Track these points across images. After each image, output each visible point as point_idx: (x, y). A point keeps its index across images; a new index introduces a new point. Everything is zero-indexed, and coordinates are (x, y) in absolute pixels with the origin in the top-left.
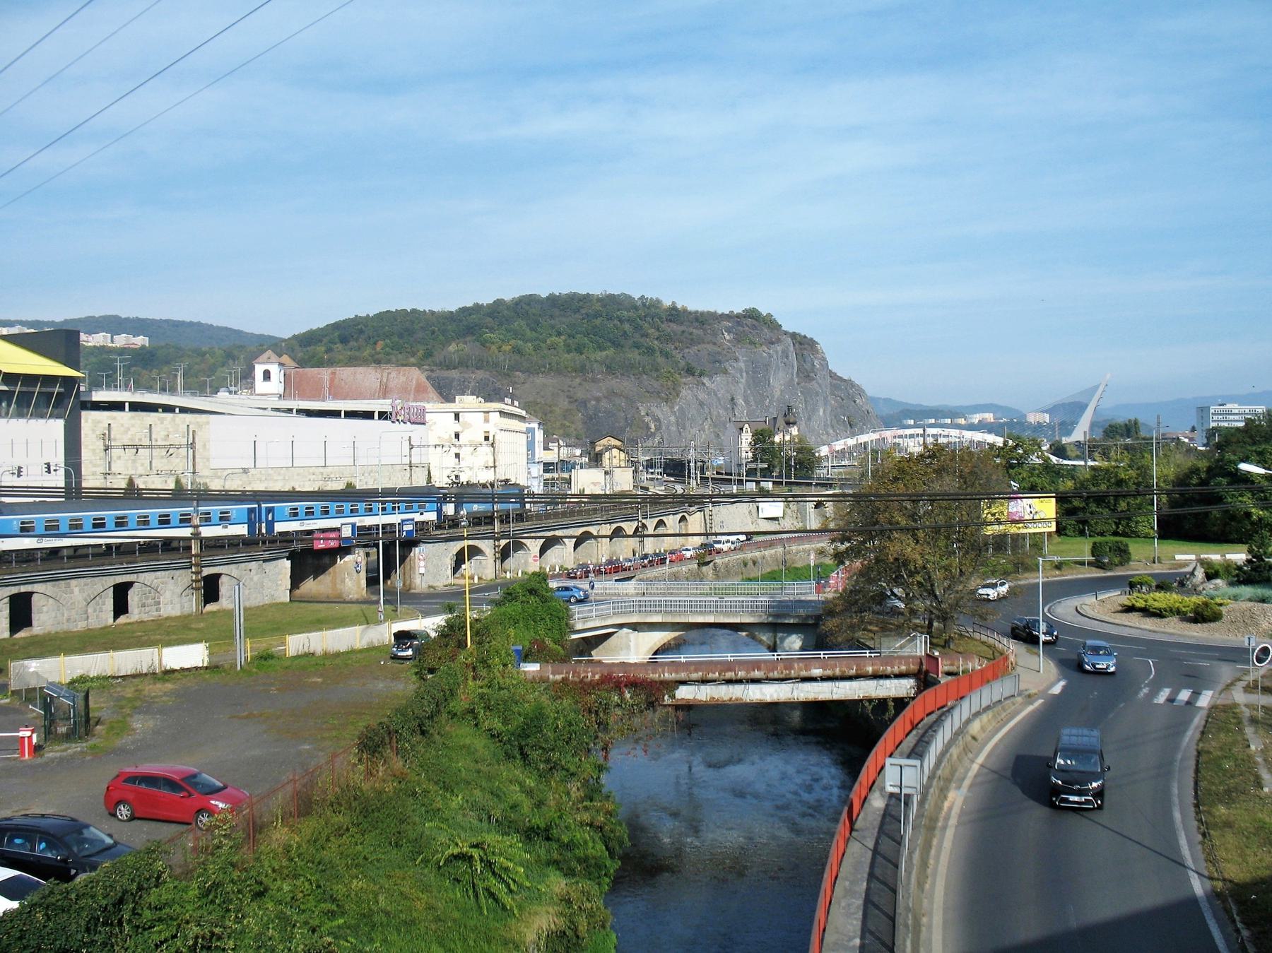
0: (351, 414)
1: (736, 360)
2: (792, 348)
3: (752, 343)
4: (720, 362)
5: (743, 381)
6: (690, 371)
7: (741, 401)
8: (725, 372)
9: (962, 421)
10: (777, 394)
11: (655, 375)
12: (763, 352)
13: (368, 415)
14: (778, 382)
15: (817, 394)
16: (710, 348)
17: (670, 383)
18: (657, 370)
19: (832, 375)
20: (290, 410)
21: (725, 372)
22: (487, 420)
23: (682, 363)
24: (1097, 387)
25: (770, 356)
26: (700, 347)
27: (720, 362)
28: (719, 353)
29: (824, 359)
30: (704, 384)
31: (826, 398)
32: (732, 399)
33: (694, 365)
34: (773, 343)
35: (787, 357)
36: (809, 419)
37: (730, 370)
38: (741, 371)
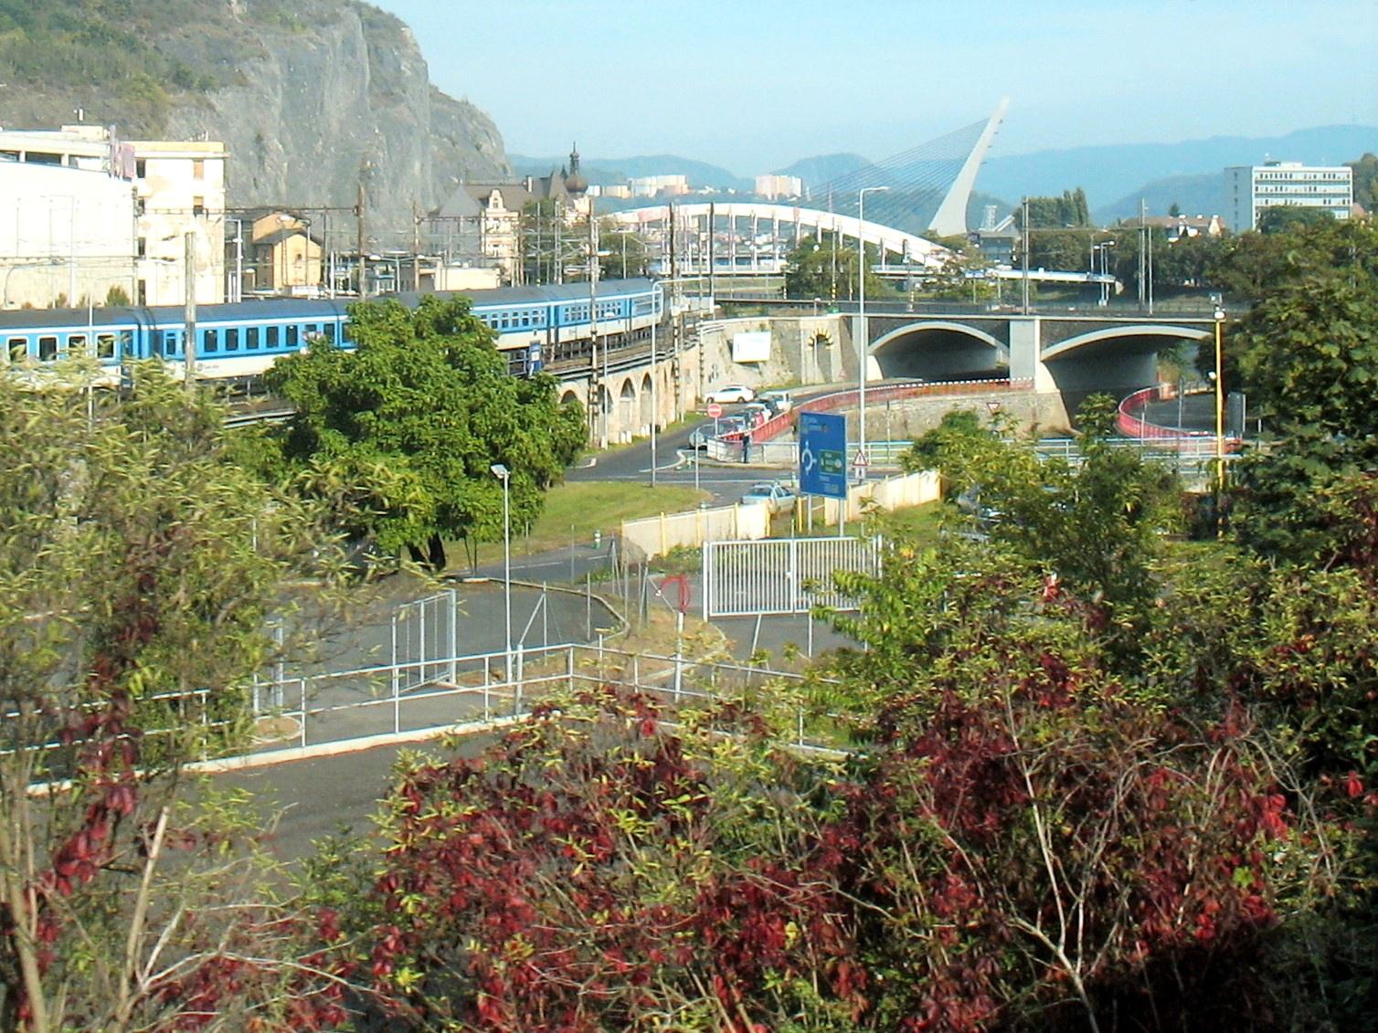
0: (34, 158)
1: (264, 57)
2: (360, 35)
3: (286, 23)
4: (230, 61)
5: (278, 100)
6: (181, 79)
7: (274, 143)
8: (242, 82)
9: (622, 192)
10: (335, 127)
11: (113, 85)
12: (307, 38)
13: (55, 159)
14: (338, 98)
15: (410, 131)
16: (209, 29)
17: (145, 105)
18: (116, 75)
19: (436, 95)
20: (16, 155)
21: (242, 82)
22: (198, 174)
23: (165, 67)
24: (984, 123)
25: (324, 51)
26: (192, 27)
27: (230, 61)
28: (229, 43)
29: (418, 58)
30: (211, 107)
31: (425, 140)
32: (259, 139)
33: (186, 67)
34: (324, 24)
35: (353, 53)
36: (395, 182)
37: (252, 78)
38: (274, 79)
